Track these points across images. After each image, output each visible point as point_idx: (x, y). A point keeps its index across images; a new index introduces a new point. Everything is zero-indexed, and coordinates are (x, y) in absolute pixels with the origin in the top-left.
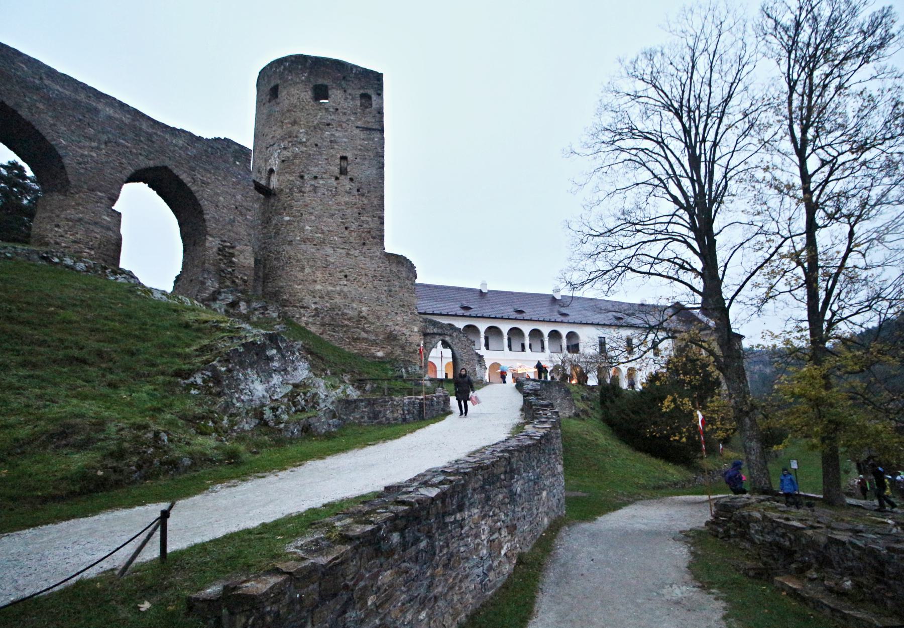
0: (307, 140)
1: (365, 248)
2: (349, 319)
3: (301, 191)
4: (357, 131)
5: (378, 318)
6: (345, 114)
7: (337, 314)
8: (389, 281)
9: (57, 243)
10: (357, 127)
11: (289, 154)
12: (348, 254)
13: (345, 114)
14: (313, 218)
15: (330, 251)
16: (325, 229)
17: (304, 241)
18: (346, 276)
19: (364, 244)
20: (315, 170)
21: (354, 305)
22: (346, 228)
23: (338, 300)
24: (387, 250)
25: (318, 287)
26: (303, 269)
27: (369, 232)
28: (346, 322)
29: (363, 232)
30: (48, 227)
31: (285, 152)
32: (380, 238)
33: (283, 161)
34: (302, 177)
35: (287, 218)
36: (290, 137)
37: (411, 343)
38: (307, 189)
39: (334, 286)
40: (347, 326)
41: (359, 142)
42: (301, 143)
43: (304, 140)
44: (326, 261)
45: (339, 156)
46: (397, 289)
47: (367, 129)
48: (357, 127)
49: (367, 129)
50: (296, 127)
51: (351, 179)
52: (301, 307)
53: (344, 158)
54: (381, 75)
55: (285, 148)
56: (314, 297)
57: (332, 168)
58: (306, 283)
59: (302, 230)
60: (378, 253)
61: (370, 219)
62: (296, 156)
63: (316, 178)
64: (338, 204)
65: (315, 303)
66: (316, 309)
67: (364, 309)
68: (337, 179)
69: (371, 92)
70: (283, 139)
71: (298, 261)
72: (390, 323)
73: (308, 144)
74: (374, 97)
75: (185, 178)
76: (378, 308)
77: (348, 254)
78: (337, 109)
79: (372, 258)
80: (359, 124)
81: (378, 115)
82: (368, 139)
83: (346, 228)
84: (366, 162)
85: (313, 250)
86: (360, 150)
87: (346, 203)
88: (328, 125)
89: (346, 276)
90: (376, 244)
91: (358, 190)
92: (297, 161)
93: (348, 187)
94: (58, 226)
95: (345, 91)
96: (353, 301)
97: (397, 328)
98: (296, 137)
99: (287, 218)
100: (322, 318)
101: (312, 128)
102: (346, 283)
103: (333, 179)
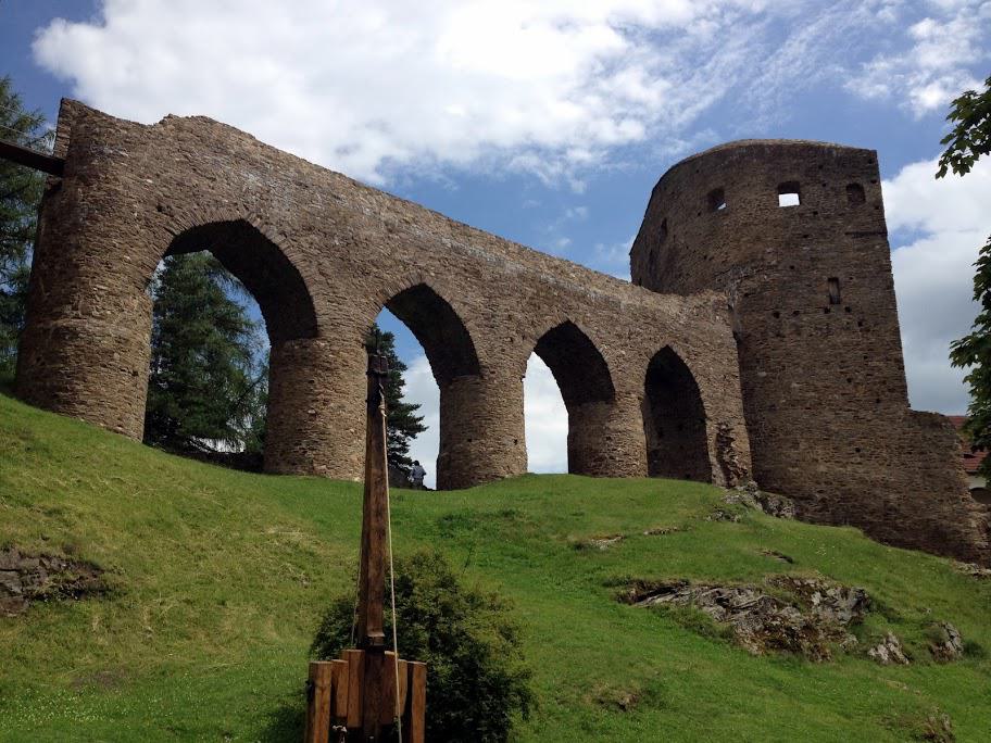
0: (778, 262)
1: (881, 407)
2: (872, 513)
3: (778, 335)
4: (847, 240)
5: (915, 509)
6: (828, 217)
7: (854, 506)
8: (922, 453)
9: (611, 458)
10: (847, 234)
11: (755, 285)
12: (857, 417)
13: (828, 217)
14: (801, 371)
15: (830, 416)
16: (819, 384)
17: (793, 404)
18: (858, 450)
19: (878, 401)
20: (795, 303)
21: (878, 492)
22: (849, 380)
23: (852, 486)
24: (914, 408)
25: (822, 468)
26: (796, 445)
27: (884, 383)
28: (868, 518)
29: (875, 384)
30: (600, 440)
31: (748, 283)
32: (902, 389)
33: (746, 295)
34: (777, 315)
35: (764, 374)
36: (753, 261)
37: (970, 545)
38: (788, 331)
39: (844, 466)
40: (871, 523)
41: (851, 255)
42: (771, 267)
43: (774, 262)
44: (827, 430)
45: (825, 278)
46: (938, 464)
47: (862, 235)
48: (847, 234)
49: (862, 235)
50: (760, 246)
51: (848, 310)
52: (801, 499)
53: (833, 280)
54: (874, 153)
55: (747, 277)
56: (818, 483)
57: (819, 296)
58: (804, 464)
59: (788, 390)
60: (901, 413)
61: (881, 364)
62: (764, 286)
63: (796, 313)
64: (834, 346)
65: (820, 492)
66: (823, 500)
67: (892, 496)
68: (827, 311)
69: (859, 181)
70: (742, 264)
71: (787, 433)
72: (934, 517)
73: (780, 268)
74: (866, 187)
75: (682, 354)
76: (911, 494)
77: (857, 417)
78: (816, 213)
79: (892, 421)
80: (849, 228)
81: (876, 212)
82: (866, 249)
83: (849, 380)
84: (867, 281)
85: (805, 416)
86: (856, 265)
87: (845, 344)
88: (806, 236)
89: (858, 450)
90: (896, 400)
91: (860, 324)
92: (767, 294)
93: (845, 320)
94: (609, 438)
95: (824, 185)
96: (874, 486)
97: (944, 522)
98: (763, 259)
99: (764, 374)
100: (833, 514)
101: (783, 245)
102: (859, 460)
103: (822, 312)
